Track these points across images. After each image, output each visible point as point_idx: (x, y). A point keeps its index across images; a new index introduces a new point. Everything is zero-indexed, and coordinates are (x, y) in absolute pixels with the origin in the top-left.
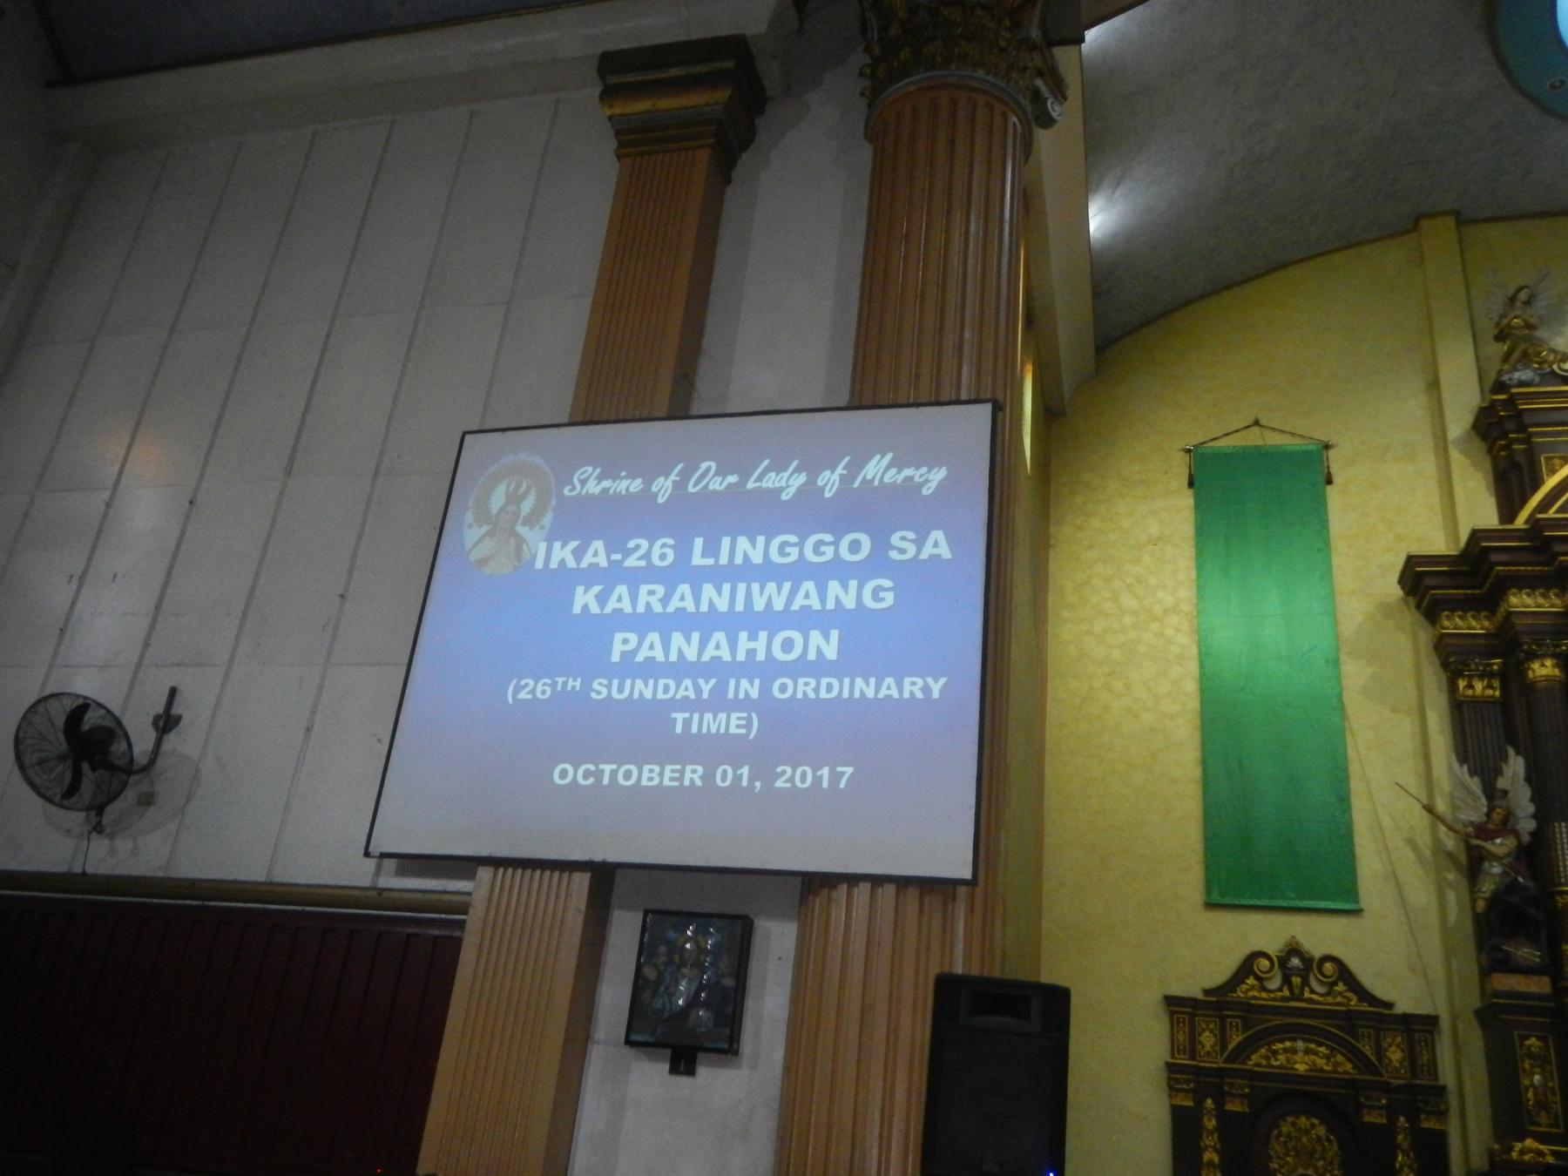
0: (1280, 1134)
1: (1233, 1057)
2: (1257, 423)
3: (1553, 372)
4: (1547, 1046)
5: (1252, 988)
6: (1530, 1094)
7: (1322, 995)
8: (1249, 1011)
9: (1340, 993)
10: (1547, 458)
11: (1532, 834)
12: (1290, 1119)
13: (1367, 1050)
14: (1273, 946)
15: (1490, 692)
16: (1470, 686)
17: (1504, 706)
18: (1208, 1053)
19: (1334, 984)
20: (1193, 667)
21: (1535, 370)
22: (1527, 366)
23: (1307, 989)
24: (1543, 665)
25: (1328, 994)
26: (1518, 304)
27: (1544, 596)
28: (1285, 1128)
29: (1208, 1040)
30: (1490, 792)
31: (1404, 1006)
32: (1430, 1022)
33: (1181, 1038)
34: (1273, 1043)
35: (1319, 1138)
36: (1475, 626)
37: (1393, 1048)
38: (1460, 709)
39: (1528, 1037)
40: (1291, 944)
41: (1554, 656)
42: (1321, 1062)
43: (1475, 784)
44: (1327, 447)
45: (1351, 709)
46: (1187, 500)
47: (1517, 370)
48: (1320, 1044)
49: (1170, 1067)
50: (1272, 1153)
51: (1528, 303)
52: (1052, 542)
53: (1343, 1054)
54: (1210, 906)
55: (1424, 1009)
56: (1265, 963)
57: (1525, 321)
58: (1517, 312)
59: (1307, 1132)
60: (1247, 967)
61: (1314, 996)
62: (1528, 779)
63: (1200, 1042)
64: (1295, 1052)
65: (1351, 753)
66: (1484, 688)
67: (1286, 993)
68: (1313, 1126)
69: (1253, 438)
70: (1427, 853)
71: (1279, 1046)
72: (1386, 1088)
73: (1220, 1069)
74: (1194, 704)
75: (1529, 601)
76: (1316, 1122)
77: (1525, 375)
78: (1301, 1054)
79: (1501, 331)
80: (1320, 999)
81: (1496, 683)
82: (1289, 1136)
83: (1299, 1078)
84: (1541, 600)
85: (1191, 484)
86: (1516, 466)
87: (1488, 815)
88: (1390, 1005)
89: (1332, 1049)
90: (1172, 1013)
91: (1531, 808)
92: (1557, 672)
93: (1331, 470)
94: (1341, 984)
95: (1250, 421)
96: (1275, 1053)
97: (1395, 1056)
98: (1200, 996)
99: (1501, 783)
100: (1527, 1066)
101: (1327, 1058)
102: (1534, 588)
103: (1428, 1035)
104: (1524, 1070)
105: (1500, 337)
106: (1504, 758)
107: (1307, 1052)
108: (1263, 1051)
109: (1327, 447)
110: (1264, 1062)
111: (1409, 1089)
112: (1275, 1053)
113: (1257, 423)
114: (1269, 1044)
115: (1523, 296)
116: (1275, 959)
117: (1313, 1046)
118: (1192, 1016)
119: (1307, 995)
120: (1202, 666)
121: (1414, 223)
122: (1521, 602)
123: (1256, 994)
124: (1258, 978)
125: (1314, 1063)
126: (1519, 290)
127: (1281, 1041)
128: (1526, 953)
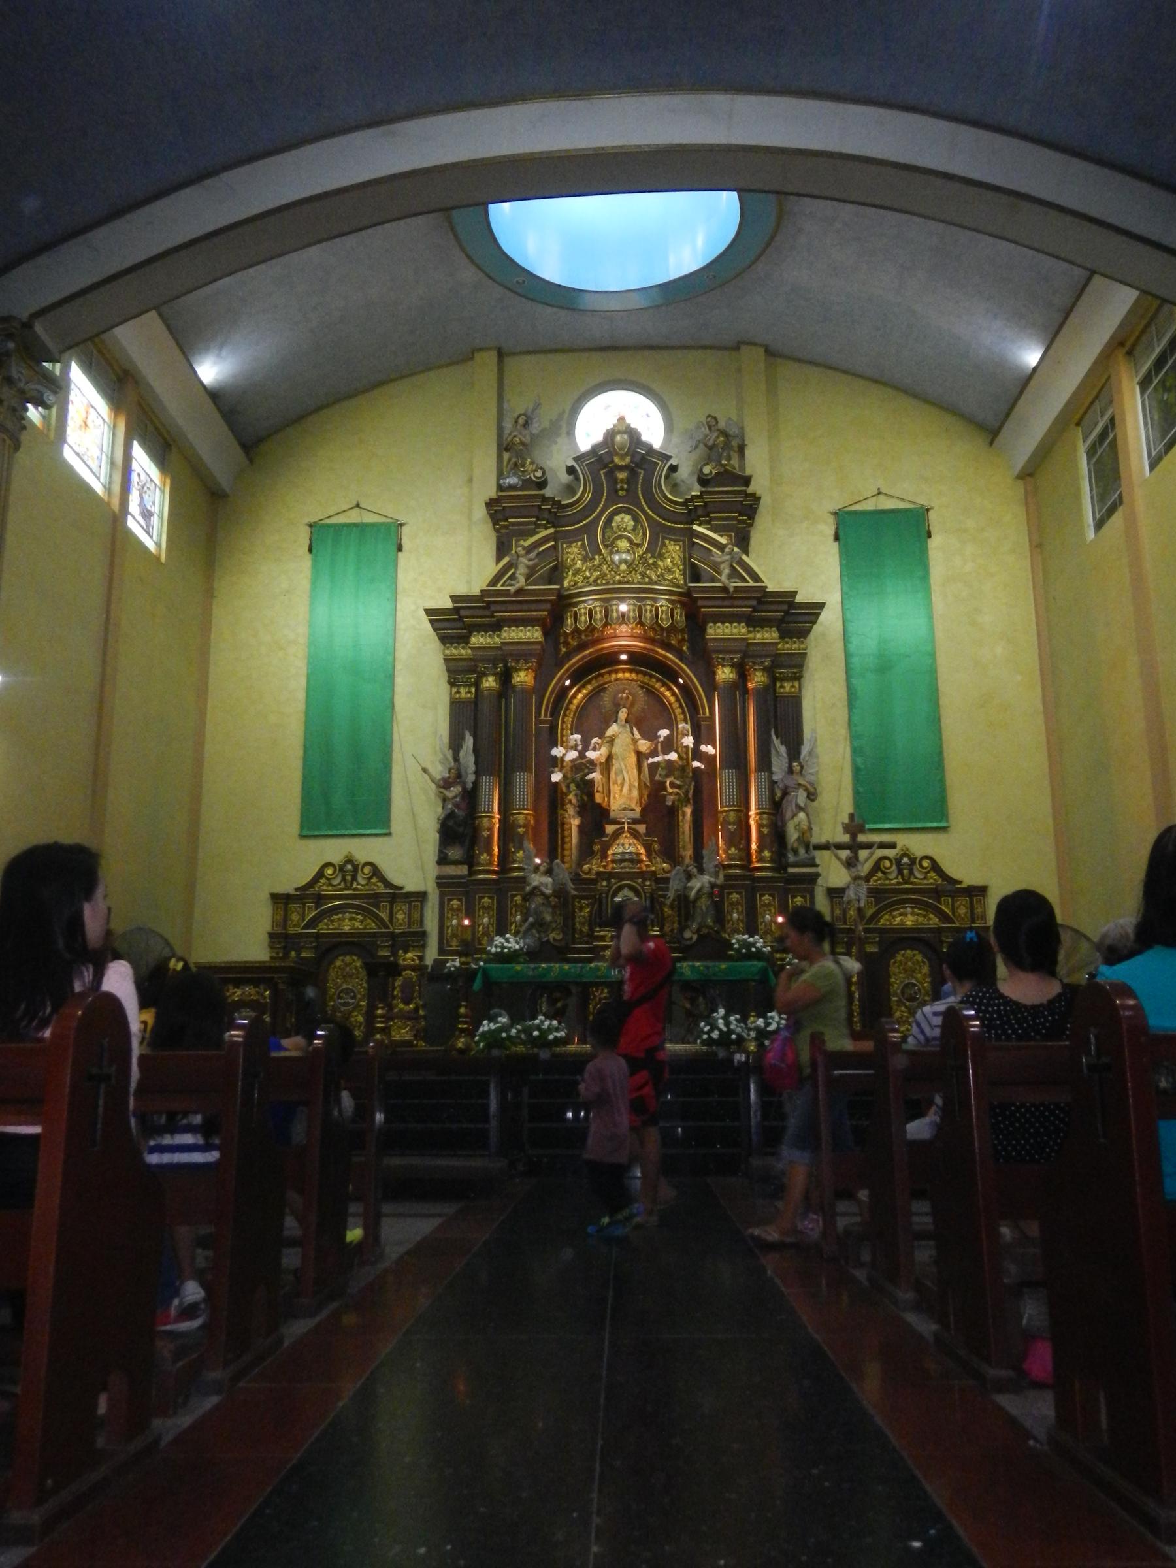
0: (335, 967)
1: (307, 927)
2: (358, 506)
3: (530, 477)
4: (462, 903)
5: (324, 884)
6: (450, 931)
7: (362, 885)
8: (319, 899)
9: (374, 884)
10: (516, 541)
11: (473, 783)
12: (340, 958)
13: (384, 915)
14: (337, 859)
15: (469, 696)
16: (458, 692)
17: (476, 702)
18: (295, 926)
19: (370, 878)
20: (303, 681)
21: (519, 477)
22: (514, 475)
23: (355, 883)
24: (487, 681)
25: (367, 884)
26: (519, 427)
27: (490, 636)
28: (338, 963)
29: (295, 917)
30: (456, 759)
31: (411, 886)
32: (421, 896)
33: (279, 918)
34: (332, 915)
35: (356, 968)
36: (463, 652)
37: (401, 912)
38: (456, 707)
39: (452, 900)
40: (347, 857)
41: (494, 674)
42: (357, 924)
43: (449, 755)
44: (401, 525)
45: (397, 708)
46: (307, 562)
47: (508, 477)
48: (358, 914)
49: (271, 935)
50: (330, 978)
51: (526, 425)
52: (216, 593)
53: (370, 919)
54: (302, 837)
55: (421, 888)
56: (330, 871)
57: (520, 439)
58: (515, 434)
59: (351, 964)
60: (320, 874)
61: (359, 887)
62: (476, 751)
63: (291, 919)
64: (344, 919)
65: (396, 737)
66: (466, 693)
67: (343, 885)
68: (354, 960)
69: (354, 517)
70: (433, 796)
71: (336, 917)
72: (393, 936)
73: (300, 934)
74: (302, 706)
75: (482, 640)
76: (355, 958)
77: (513, 480)
78: (347, 920)
79: (508, 445)
80: (362, 888)
81: (473, 690)
82: (339, 967)
83: (346, 935)
84: (489, 640)
85: (310, 551)
86: (503, 543)
87: (449, 772)
88: (401, 888)
89: (365, 916)
90: (275, 903)
91: (472, 768)
92: (493, 684)
93: (403, 542)
94: (374, 878)
95: (354, 503)
96: (332, 921)
97: (400, 916)
98: (292, 892)
99: (462, 753)
100: (450, 915)
101: (362, 922)
102: (486, 632)
103: (419, 904)
104: (448, 918)
105: (507, 450)
106: (463, 738)
107: (351, 919)
108: (326, 921)
109: (401, 525)
110: (325, 927)
111: (403, 934)
112: (332, 921)
113: (358, 506)
114: (329, 916)
115: (521, 421)
116: (338, 868)
117: (354, 915)
118: (286, 904)
119: (355, 885)
120: (308, 682)
121: (468, 357)
122: (477, 640)
123: (325, 887)
124: (327, 879)
125: (354, 924)
126: (519, 416)
127: (337, 914)
128: (455, 853)
